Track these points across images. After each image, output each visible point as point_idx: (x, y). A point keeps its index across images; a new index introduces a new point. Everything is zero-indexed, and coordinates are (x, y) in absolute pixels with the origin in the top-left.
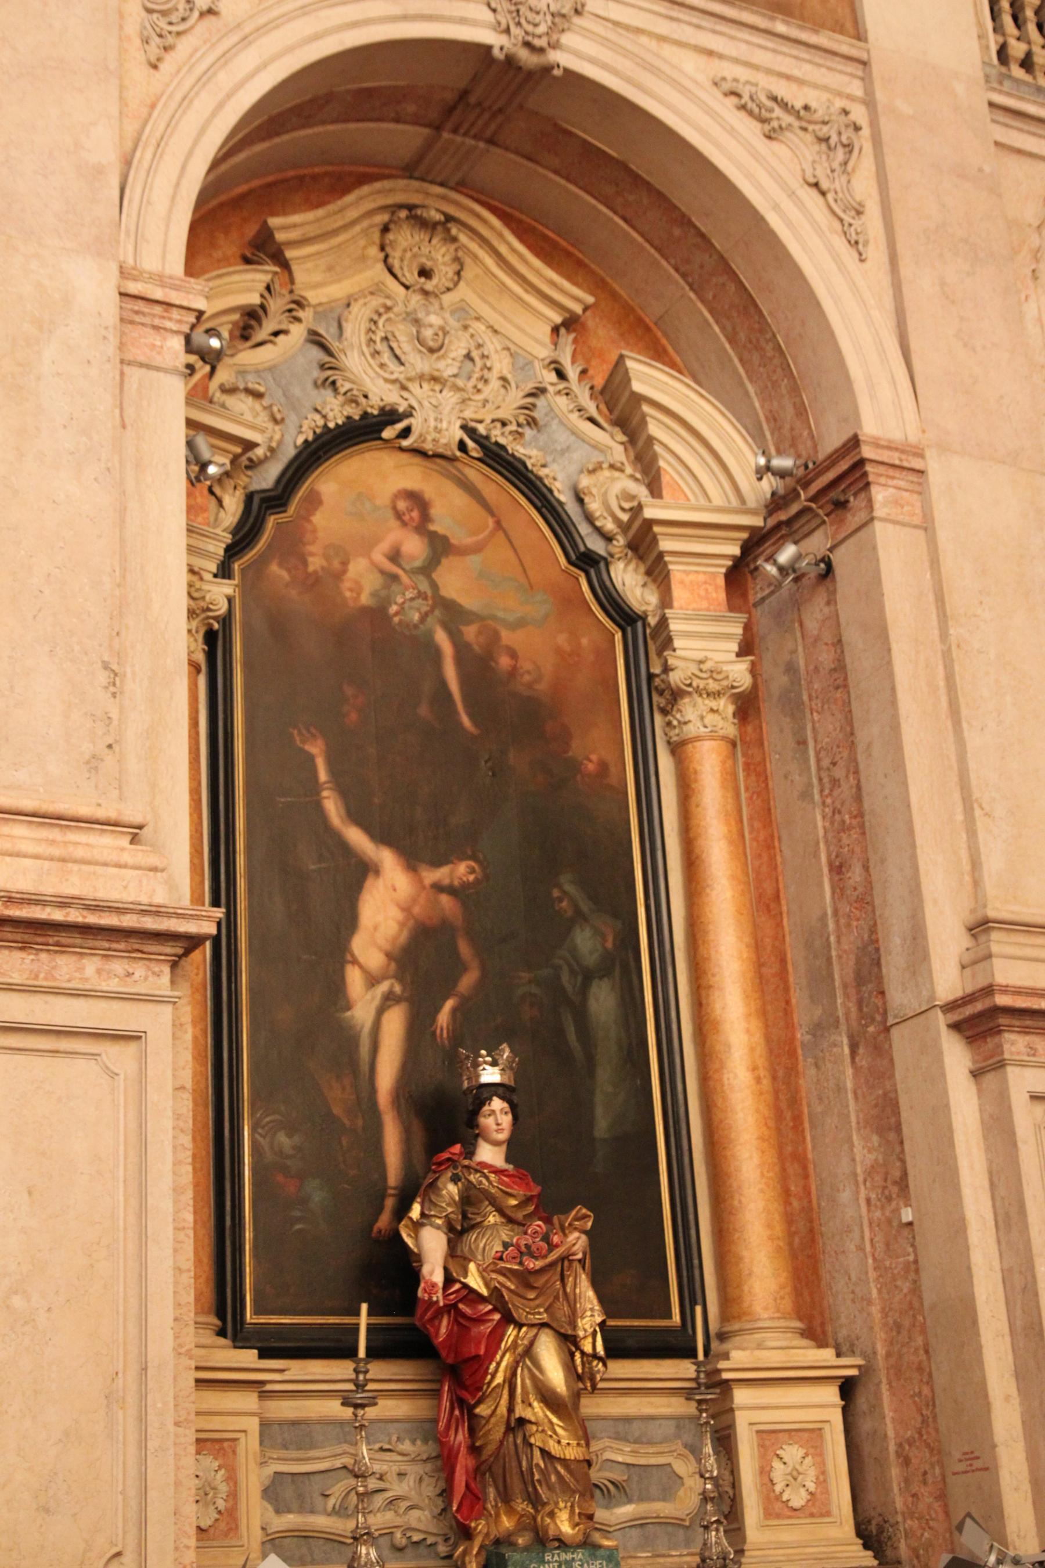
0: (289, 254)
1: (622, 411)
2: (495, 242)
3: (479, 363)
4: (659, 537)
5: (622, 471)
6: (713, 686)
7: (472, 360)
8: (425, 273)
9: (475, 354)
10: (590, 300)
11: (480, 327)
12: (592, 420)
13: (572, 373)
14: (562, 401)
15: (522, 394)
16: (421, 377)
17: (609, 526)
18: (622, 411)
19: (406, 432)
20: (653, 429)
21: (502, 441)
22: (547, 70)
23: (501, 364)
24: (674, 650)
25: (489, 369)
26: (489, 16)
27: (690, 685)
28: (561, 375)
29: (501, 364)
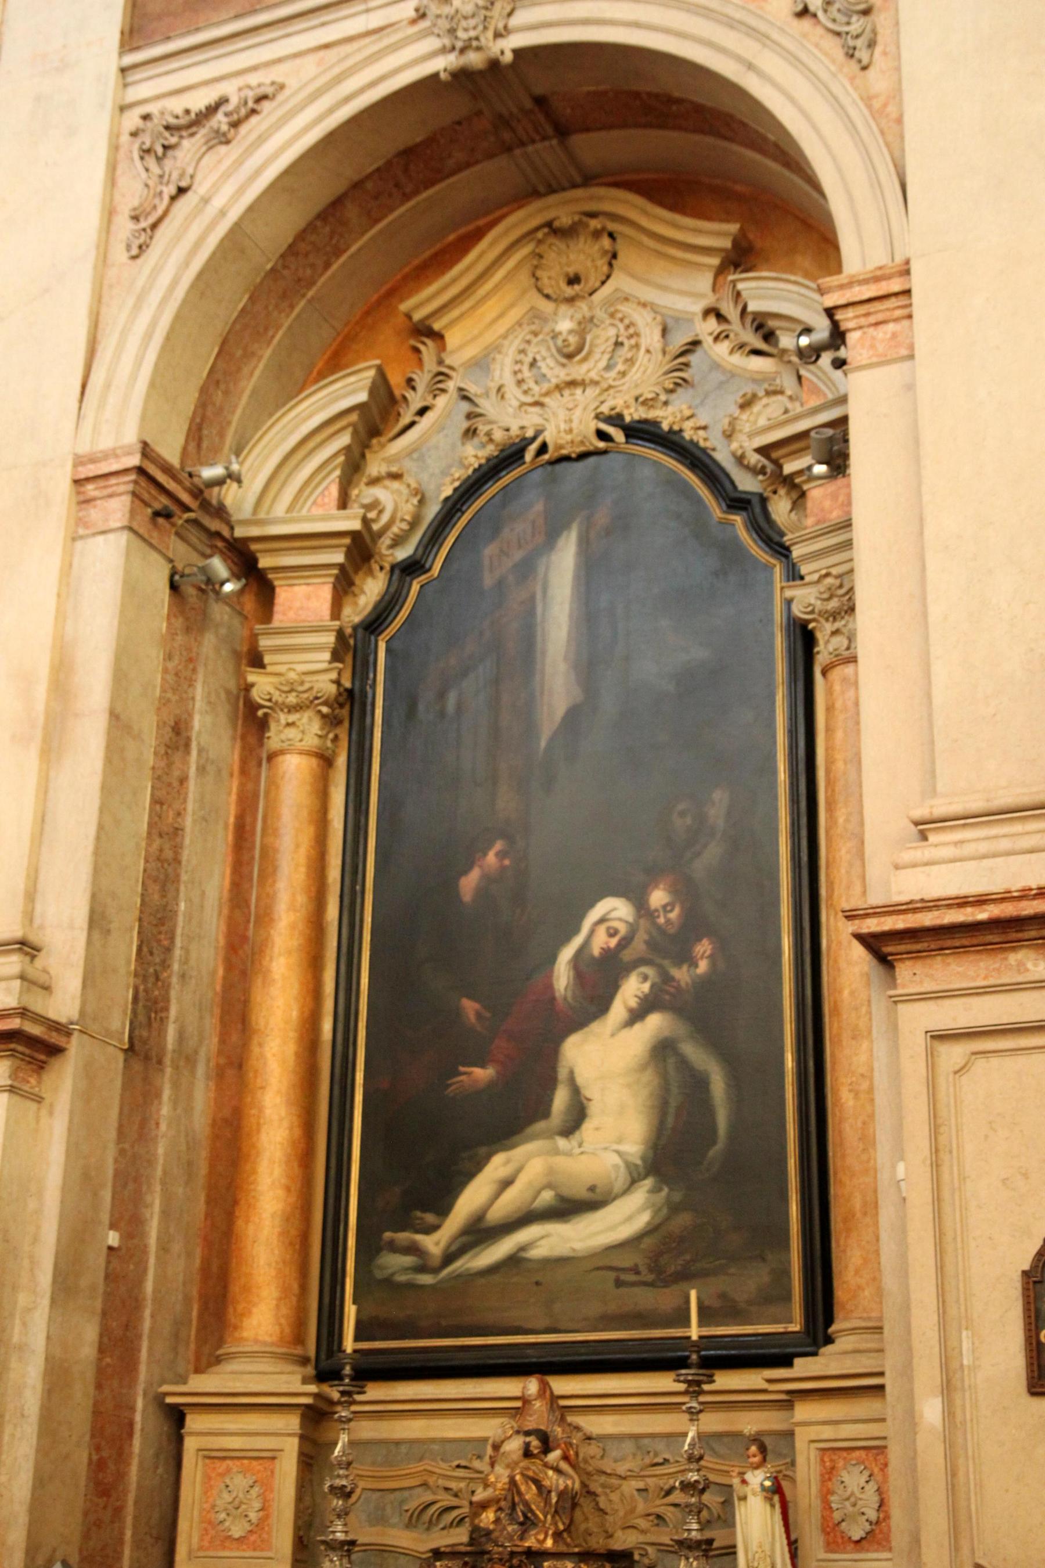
0: (437, 326)
4: (258, 555)
5: (781, 392)
8: (574, 280)
10: (734, 228)
11: (625, 308)
15: (668, 357)
19: (543, 449)
21: (636, 417)
22: (494, 65)
23: (651, 337)
24: (802, 578)
25: (637, 346)
27: (812, 612)
28: (720, 317)
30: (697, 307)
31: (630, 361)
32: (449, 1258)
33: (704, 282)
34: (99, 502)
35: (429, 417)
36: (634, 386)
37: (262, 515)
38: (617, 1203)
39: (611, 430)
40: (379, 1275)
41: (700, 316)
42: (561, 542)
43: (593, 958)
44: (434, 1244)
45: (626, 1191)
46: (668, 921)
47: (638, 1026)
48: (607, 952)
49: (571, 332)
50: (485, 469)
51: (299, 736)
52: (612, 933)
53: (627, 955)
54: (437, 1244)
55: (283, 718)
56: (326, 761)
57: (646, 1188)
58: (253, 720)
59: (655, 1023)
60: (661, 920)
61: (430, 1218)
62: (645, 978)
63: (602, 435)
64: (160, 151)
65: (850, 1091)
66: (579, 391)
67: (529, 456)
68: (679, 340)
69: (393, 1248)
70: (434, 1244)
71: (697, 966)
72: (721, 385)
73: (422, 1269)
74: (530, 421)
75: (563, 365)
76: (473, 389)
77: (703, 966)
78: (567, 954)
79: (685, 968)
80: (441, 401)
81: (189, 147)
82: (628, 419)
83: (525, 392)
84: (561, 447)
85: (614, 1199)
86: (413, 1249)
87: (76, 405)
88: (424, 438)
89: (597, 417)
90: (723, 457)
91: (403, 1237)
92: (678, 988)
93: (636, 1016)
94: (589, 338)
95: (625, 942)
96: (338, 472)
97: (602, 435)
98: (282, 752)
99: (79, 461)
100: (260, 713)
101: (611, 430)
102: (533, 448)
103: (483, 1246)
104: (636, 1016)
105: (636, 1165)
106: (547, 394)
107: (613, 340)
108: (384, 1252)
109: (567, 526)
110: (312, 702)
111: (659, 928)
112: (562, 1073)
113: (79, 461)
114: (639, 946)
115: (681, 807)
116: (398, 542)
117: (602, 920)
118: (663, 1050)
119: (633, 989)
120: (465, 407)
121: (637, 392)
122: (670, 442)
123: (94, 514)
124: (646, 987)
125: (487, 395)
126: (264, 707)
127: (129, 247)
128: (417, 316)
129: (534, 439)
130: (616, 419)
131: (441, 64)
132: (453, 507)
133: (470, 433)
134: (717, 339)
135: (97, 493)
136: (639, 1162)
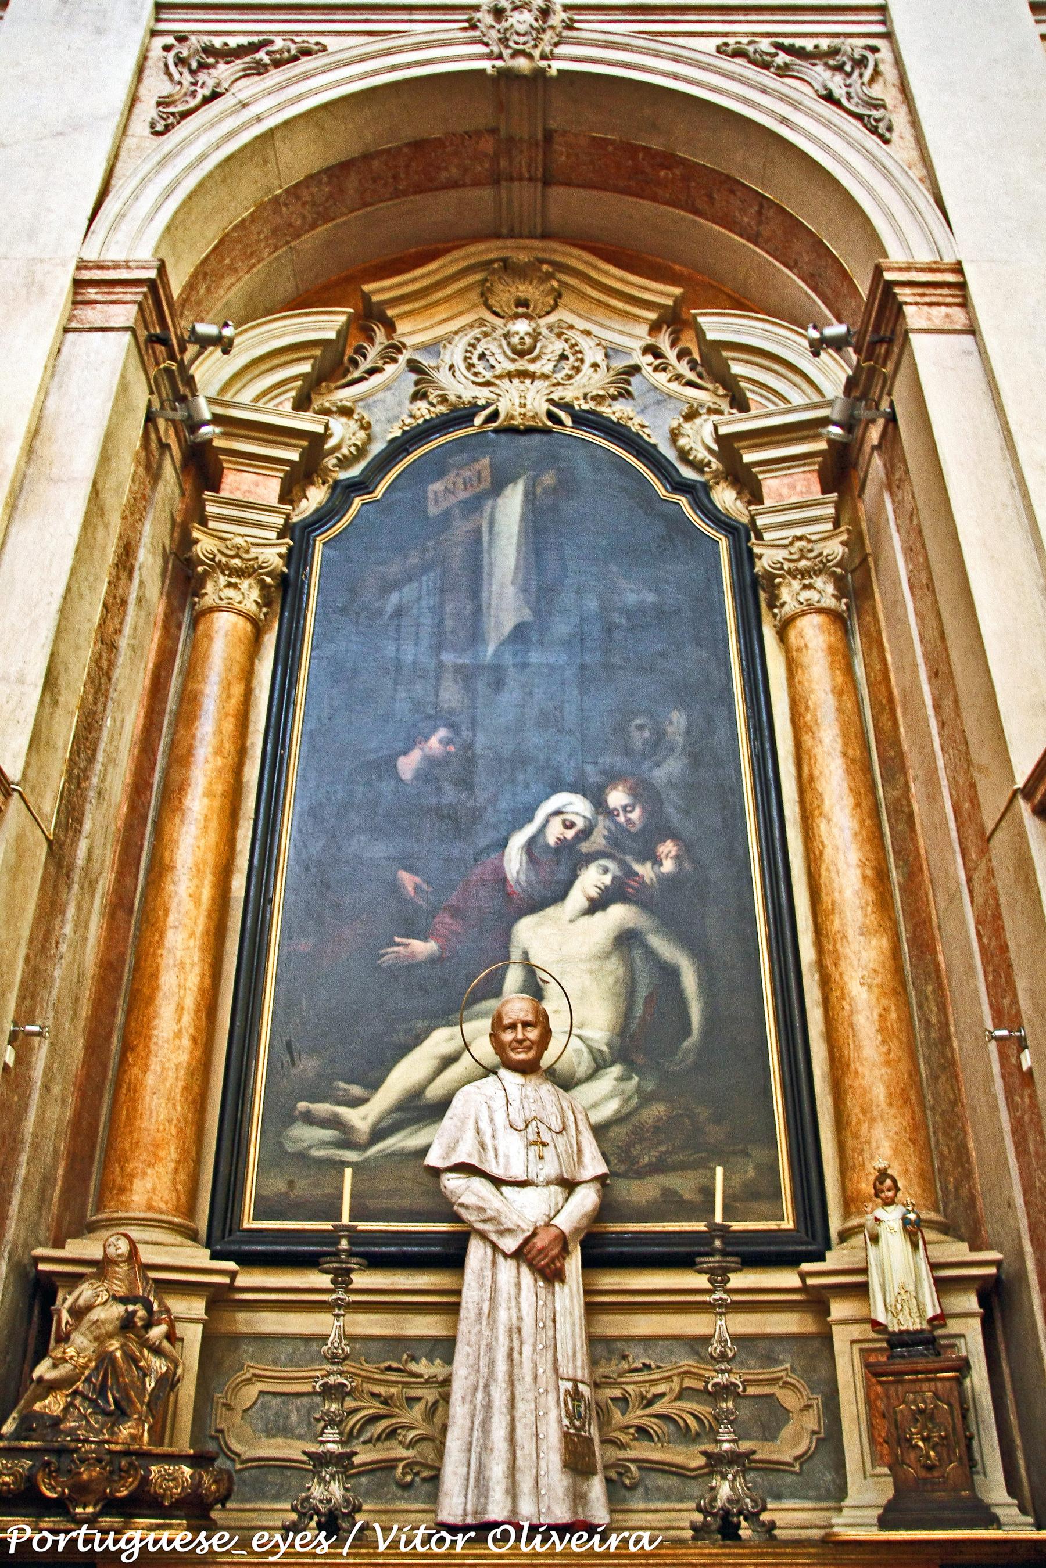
1: (713, 364)
2: (593, 274)
3: (572, 358)
6: (803, 564)
7: (567, 358)
9: (568, 353)
10: (678, 291)
12: (690, 384)
13: (671, 355)
14: (662, 378)
15: (612, 372)
16: (510, 375)
17: (702, 454)
18: (713, 364)
19: (494, 416)
20: (736, 369)
25: (582, 361)
26: (485, 50)
29: (593, 354)
30: (637, 345)
31: (578, 370)
32: (378, 1134)
33: (643, 330)
34: (98, 306)
35: (376, 379)
36: (585, 386)
37: (227, 397)
38: (580, 1088)
39: (562, 415)
40: (291, 1148)
41: (640, 352)
42: (508, 491)
43: (547, 845)
44: (361, 1119)
45: (590, 1078)
46: (628, 820)
47: (599, 915)
48: (562, 841)
49: (527, 334)
50: (437, 421)
51: (239, 598)
52: (569, 825)
53: (585, 847)
54: (364, 1118)
55: (223, 580)
56: (258, 630)
57: (615, 1075)
58: (185, 577)
59: (619, 915)
60: (621, 819)
61: (356, 1090)
62: (606, 871)
63: (550, 415)
64: (194, 65)
65: (862, 984)
66: (528, 381)
67: (478, 420)
68: (619, 364)
69: (309, 1119)
70: (361, 1119)
71: (661, 865)
72: (658, 402)
73: (347, 1143)
74: (483, 395)
75: (513, 361)
76: (426, 361)
77: (668, 866)
78: (519, 840)
79: (649, 865)
80: (390, 369)
81: (223, 72)
82: (577, 408)
83: (476, 374)
84: (512, 418)
85: (577, 1085)
86: (335, 1122)
87: (87, 223)
88: (371, 393)
89: (550, 401)
90: (670, 453)
91: (322, 1108)
92: (643, 883)
93: (596, 906)
94: (539, 345)
95: (586, 833)
96: (293, 393)
97: (550, 415)
98: (212, 610)
99: (82, 265)
100: (200, 569)
101: (562, 415)
102: (484, 414)
103: (413, 1128)
104: (596, 906)
105: (600, 1051)
106: (499, 377)
107: (560, 352)
108: (299, 1123)
109: (514, 480)
110: (255, 571)
111: (618, 825)
112: (516, 955)
113: (82, 265)
114: (598, 840)
115: (638, 721)
116: (344, 463)
117: (558, 813)
118: (626, 940)
119: (592, 879)
120: (414, 377)
121: (586, 391)
122: (617, 432)
123: (92, 315)
124: (607, 879)
125: (438, 368)
126: (203, 563)
127: (152, 125)
128: (376, 298)
129: (484, 408)
130: (567, 407)
131: (487, 65)
132: (399, 448)
133: (419, 396)
134: (656, 369)
135: (99, 297)
136: (605, 1049)
